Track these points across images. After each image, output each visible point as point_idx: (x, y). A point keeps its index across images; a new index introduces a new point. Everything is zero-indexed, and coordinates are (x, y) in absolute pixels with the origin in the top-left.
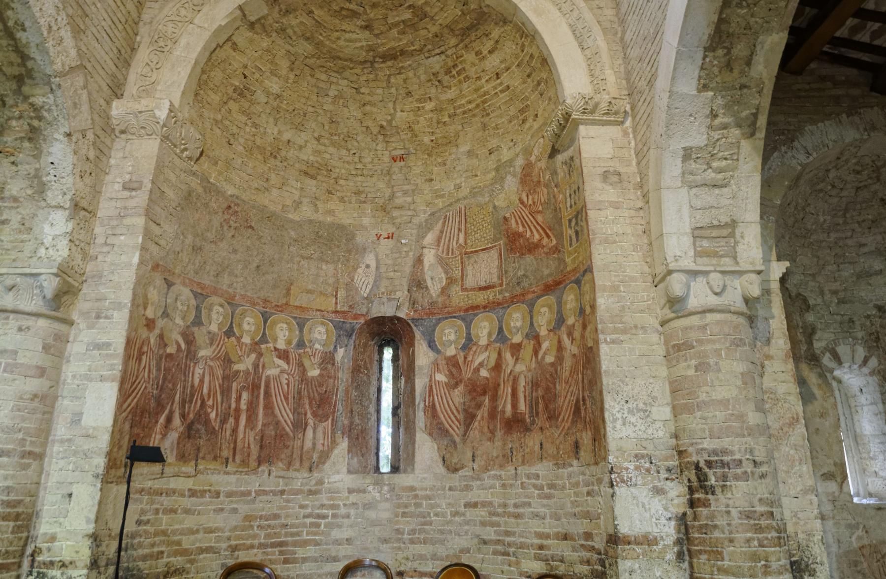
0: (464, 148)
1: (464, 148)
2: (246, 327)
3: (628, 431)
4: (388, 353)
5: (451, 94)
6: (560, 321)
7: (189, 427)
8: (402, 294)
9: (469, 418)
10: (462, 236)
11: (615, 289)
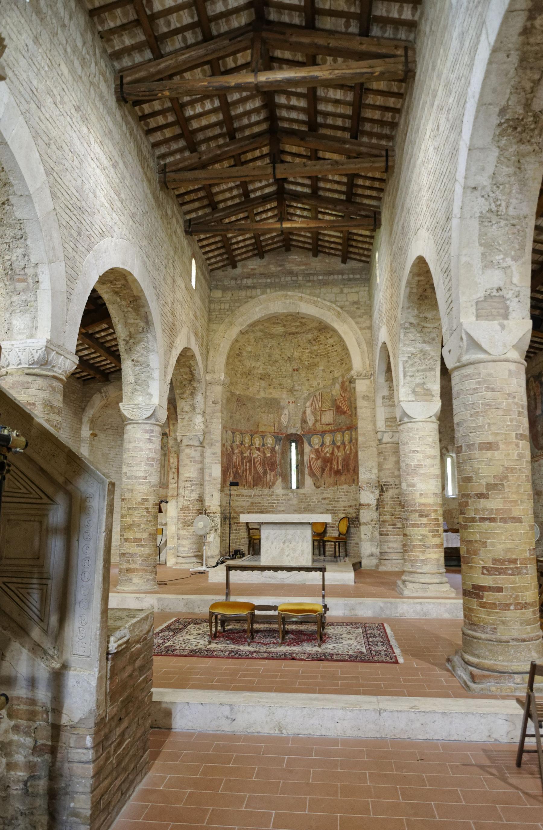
0: (321, 368)
1: (321, 368)
3: (365, 476)
4: (293, 445)
5: (315, 348)
6: (351, 441)
7: (235, 475)
8: (298, 425)
9: (323, 470)
11: (364, 434)
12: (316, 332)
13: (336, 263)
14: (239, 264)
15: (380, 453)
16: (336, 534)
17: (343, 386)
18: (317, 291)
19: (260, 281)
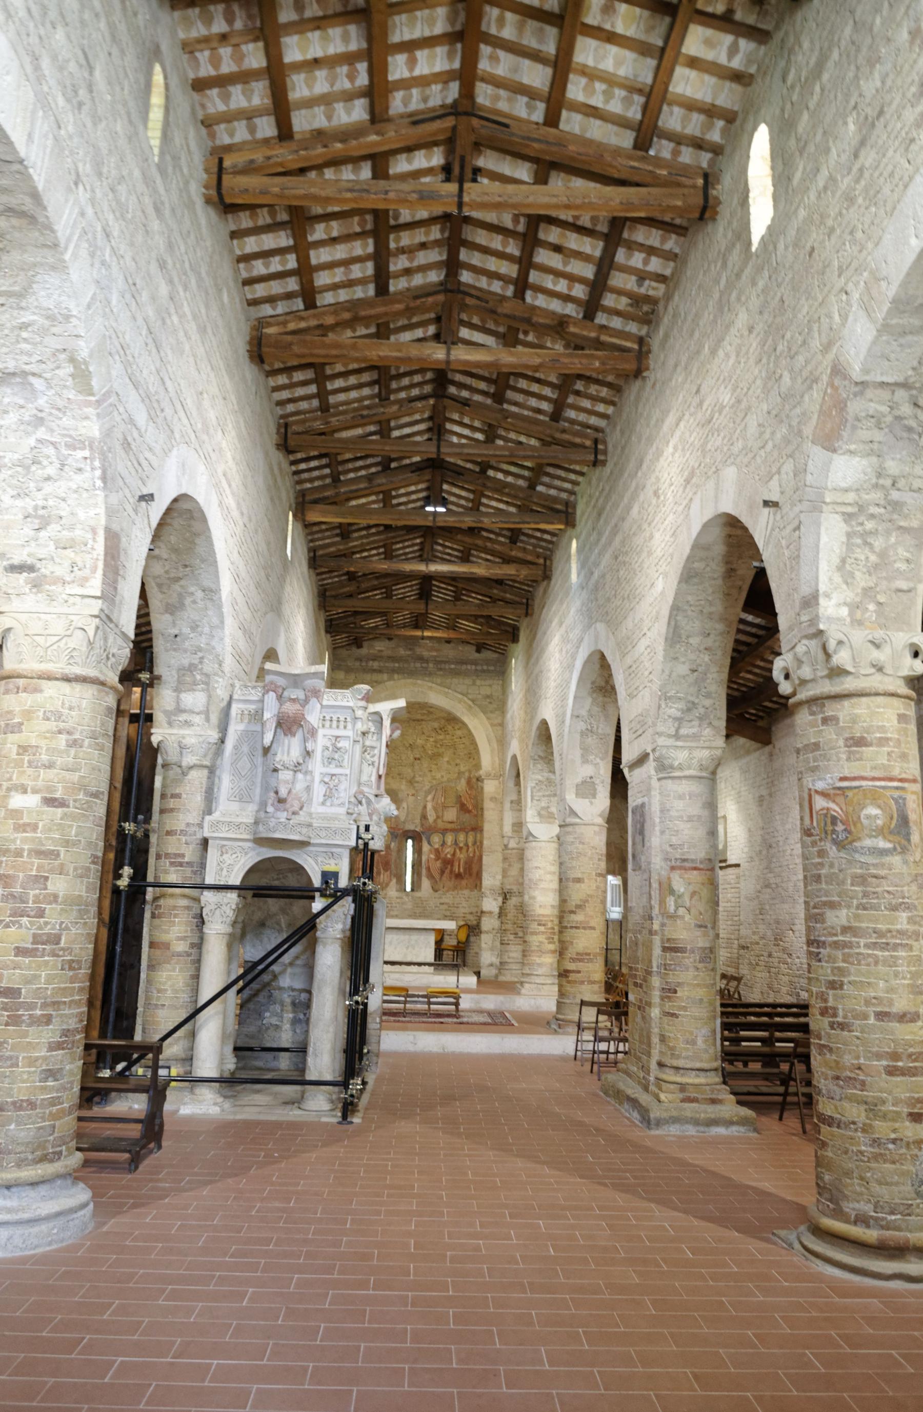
0: (446, 759)
1: (446, 759)
4: (410, 842)
5: (441, 737)
6: (475, 843)
8: (418, 821)
9: (442, 872)
12: (443, 722)
13: (470, 652)
14: (365, 644)
15: (505, 859)
16: (454, 942)
17: (469, 782)
18: (448, 681)
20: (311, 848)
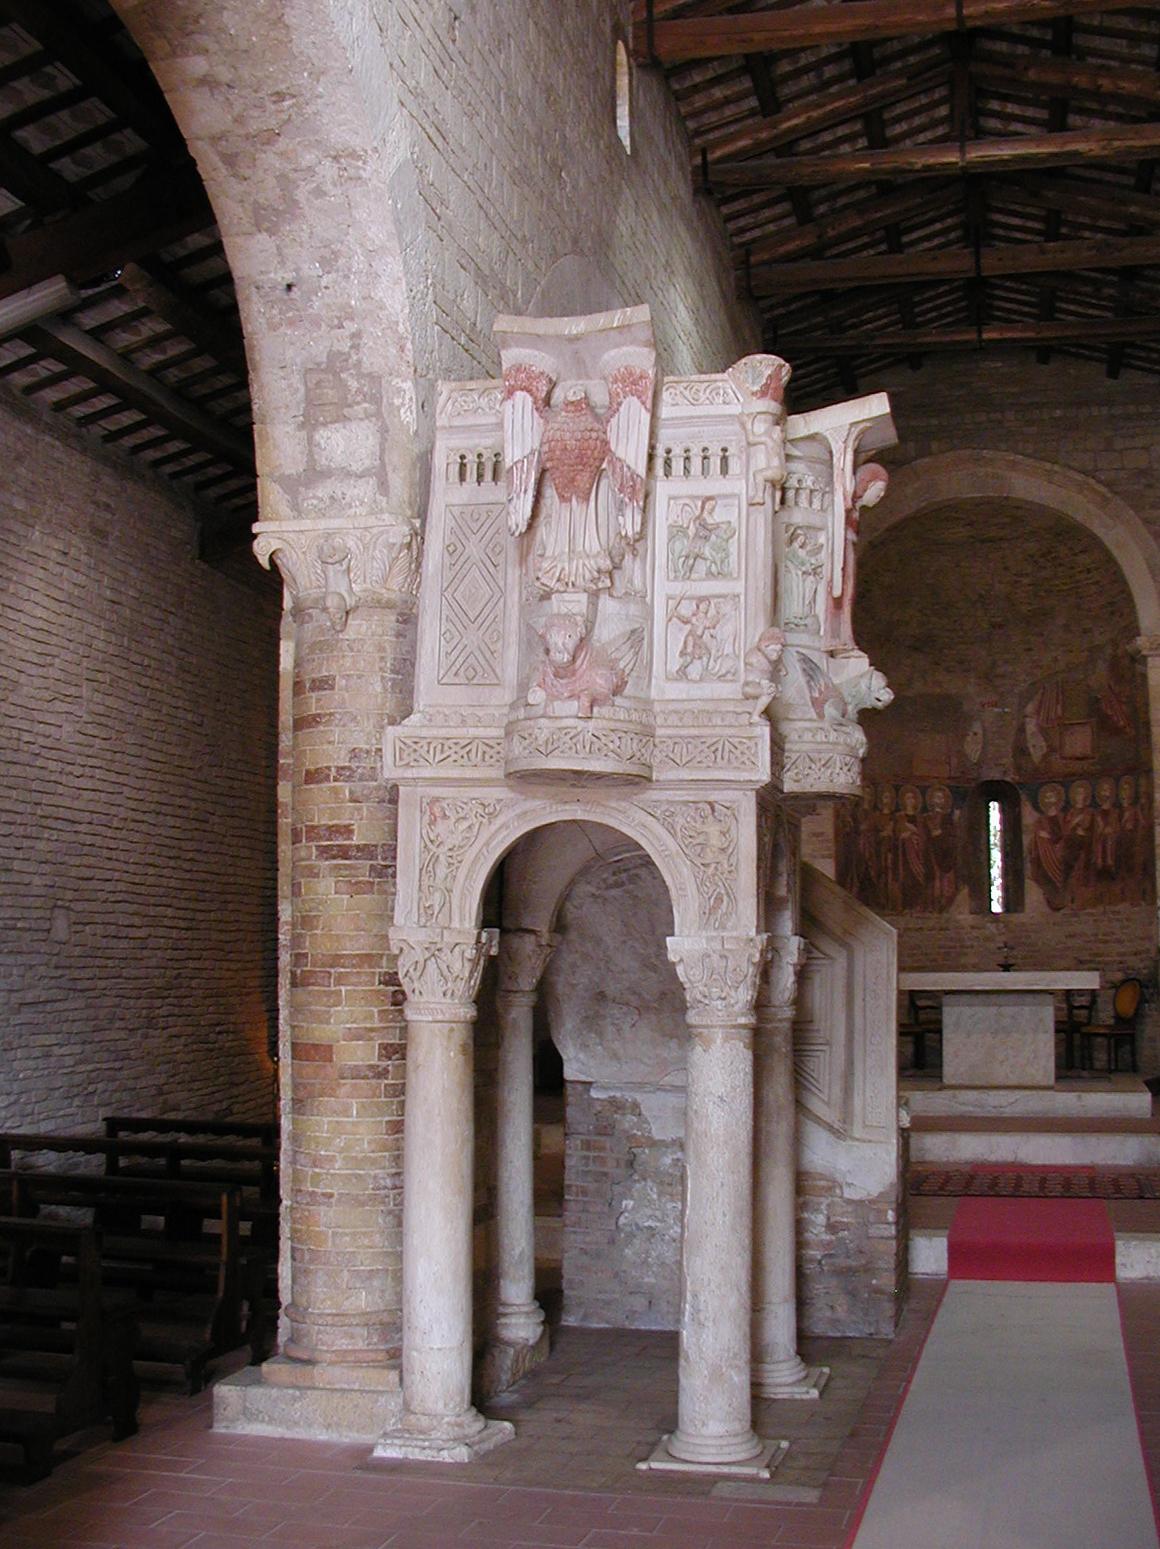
2: (885, 801)
4: (994, 808)
6: (1135, 800)
8: (1008, 761)
9: (1068, 868)
10: (1059, 707)
17: (1114, 665)
19: (913, 423)
20: (653, 795)
